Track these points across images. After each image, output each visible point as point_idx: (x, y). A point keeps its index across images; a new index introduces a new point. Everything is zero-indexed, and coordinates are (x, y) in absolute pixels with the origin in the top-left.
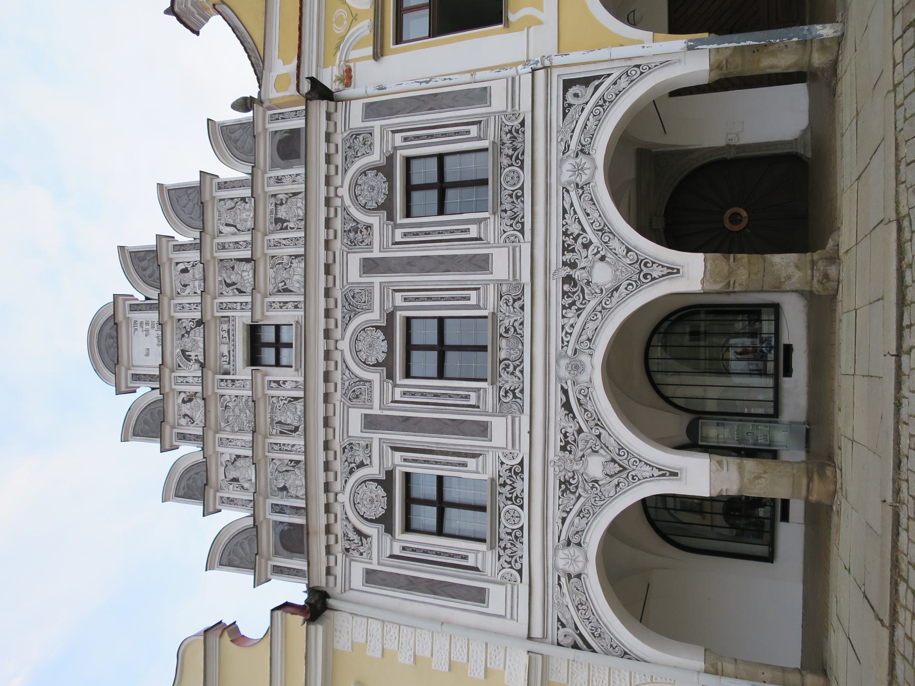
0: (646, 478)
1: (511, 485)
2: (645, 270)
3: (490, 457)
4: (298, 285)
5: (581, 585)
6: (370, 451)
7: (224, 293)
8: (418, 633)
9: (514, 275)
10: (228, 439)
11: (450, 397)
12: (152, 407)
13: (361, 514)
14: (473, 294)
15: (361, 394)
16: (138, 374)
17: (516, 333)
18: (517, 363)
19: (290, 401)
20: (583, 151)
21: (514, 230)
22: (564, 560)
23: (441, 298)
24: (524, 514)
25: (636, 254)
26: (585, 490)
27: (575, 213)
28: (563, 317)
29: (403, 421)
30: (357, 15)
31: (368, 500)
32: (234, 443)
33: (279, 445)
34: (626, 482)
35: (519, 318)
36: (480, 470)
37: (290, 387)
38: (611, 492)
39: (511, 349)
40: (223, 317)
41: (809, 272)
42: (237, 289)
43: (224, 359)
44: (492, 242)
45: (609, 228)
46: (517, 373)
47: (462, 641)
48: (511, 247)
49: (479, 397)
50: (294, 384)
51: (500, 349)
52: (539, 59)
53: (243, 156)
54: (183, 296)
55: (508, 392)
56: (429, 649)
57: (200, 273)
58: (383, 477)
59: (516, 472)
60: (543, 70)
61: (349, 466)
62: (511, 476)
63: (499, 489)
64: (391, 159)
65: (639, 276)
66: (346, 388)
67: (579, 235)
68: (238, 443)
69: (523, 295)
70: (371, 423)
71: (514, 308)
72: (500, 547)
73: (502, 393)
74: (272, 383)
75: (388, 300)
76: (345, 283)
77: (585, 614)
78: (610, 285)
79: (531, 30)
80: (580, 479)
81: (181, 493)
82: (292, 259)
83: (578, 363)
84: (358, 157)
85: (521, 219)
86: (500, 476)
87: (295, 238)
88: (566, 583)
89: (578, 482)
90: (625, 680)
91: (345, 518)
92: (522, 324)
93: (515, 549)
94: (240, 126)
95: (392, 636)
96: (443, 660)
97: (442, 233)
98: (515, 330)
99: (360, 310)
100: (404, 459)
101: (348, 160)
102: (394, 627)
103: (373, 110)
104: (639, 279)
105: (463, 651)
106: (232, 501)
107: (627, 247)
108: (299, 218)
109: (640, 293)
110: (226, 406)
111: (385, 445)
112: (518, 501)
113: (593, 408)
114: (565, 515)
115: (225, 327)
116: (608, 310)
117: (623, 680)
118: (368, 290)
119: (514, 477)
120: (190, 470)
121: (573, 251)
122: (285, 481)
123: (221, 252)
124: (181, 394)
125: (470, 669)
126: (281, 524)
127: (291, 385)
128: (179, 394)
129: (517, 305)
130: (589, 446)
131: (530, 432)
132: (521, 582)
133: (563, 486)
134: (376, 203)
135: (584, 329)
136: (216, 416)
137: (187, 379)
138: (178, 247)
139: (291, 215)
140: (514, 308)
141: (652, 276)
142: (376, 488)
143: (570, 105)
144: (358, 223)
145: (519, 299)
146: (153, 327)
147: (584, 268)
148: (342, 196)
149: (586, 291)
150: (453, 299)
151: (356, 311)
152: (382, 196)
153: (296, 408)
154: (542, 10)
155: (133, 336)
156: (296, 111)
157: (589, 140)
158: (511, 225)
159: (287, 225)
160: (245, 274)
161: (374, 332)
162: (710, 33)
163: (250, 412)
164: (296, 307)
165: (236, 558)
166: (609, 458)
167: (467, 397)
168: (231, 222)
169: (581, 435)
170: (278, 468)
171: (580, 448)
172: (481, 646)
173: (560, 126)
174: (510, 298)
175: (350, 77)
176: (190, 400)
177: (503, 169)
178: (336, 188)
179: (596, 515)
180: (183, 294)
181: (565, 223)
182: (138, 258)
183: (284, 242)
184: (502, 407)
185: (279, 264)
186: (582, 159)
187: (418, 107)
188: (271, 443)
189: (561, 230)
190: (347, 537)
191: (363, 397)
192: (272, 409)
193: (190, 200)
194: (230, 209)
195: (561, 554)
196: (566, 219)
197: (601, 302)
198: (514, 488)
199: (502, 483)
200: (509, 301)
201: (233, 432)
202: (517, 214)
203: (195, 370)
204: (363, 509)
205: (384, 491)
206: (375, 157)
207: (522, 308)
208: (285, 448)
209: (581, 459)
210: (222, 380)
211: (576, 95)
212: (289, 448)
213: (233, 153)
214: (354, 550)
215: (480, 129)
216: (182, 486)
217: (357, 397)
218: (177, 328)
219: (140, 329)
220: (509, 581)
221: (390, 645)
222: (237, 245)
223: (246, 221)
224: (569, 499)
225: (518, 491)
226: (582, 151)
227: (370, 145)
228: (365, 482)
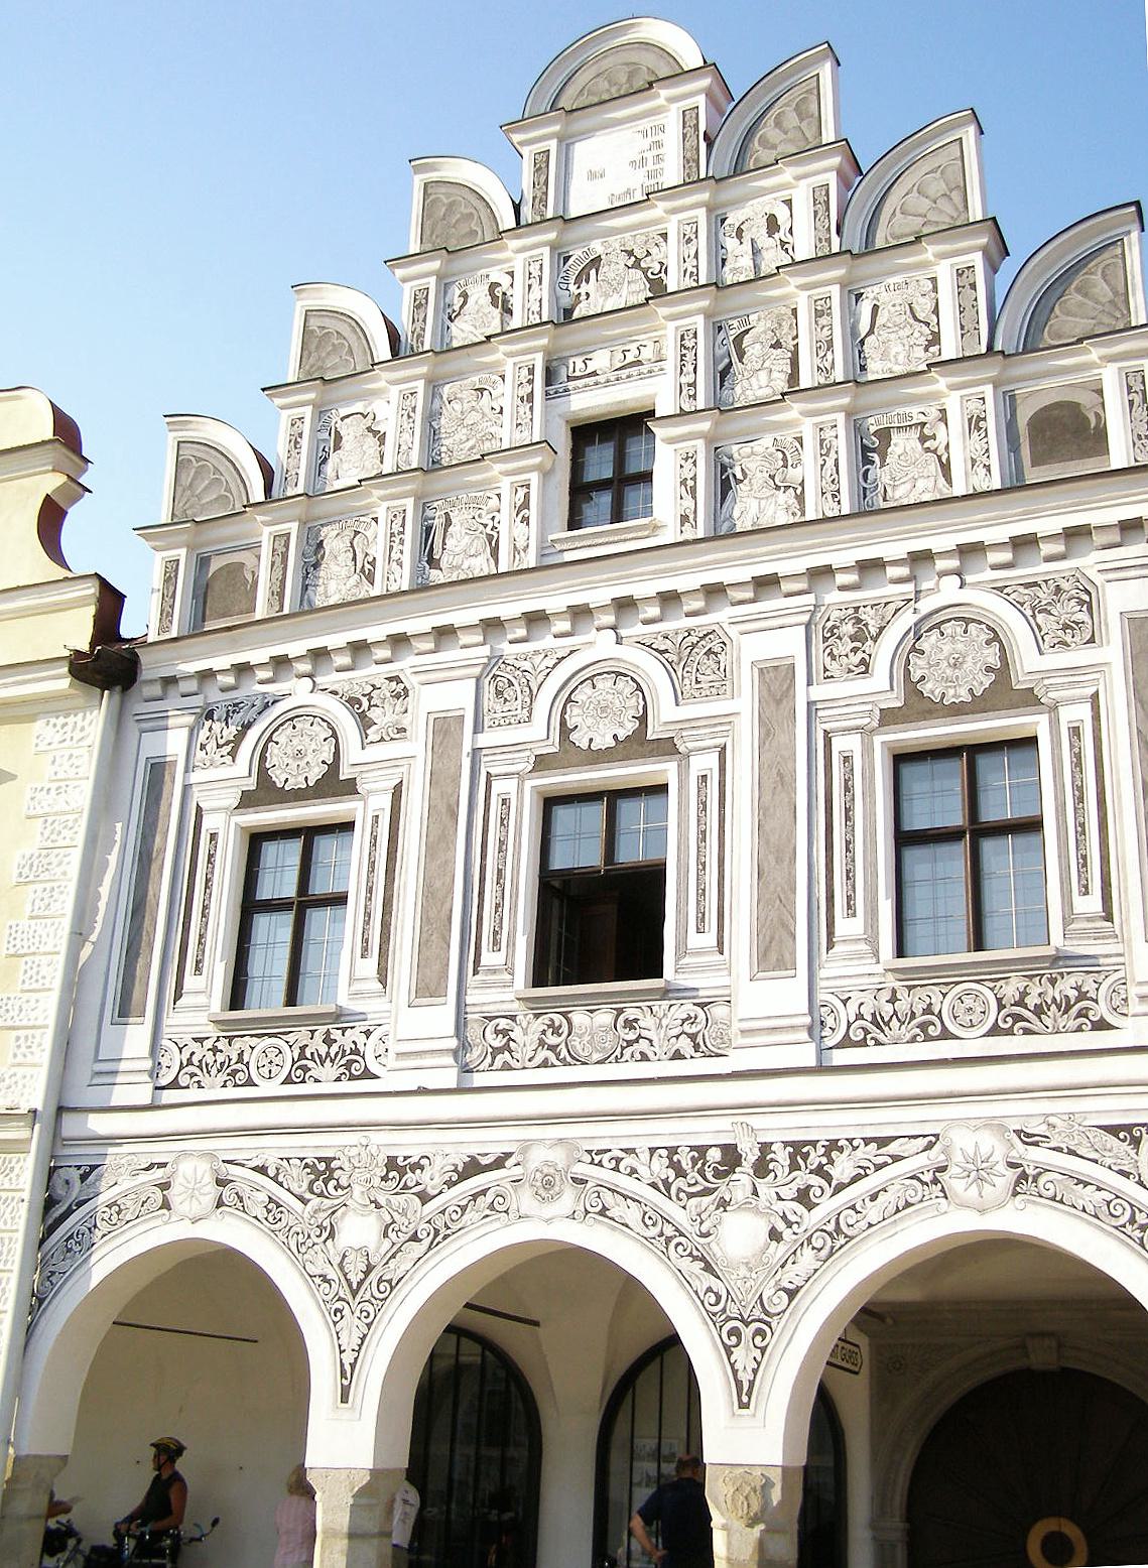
0: (339, 1338)
2: (747, 1332)
5: (151, 1210)
7: (722, 335)
11: (497, 906)
12: (484, 213)
13: (275, 735)
14: (710, 939)
17: (625, 1044)
18: (564, 1053)
20: (1023, 1179)
21: (849, 1025)
22: (192, 1174)
27: (879, 1167)
28: (652, 1150)
29: (449, 806)
36: (357, 986)
38: (313, 1269)
49: (495, 972)
58: (345, 773)
59: (353, 1066)
61: (364, 695)
64: (1029, 699)
65: (736, 1319)
67: (828, 1178)
68: (406, 436)
71: (677, 1037)
73: (503, 1023)
77: (103, 1219)
78: (719, 1254)
80: (336, 1202)
82: (795, 489)
83: (557, 1189)
85: (872, 1038)
91: (266, 701)
92: (644, 1057)
93: (214, 1071)
94: (1121, 290)
98: (630, 1043)
99: (680, 674)
101: (1026, 591)
106: (296, 442)
107: (798, 1289)
108: (889, 489)
112: (299, 1072)
113: (469, 1223)
114: (272, 1172)
116: (665, 1250)
118: (722, 684)
119: (343, 1062)
127: (521, 536)
129: (685, 1045)
130: (396, 1216)
131: (422, 1091)
133: (322, 1166)
134: (923, 678)
135: (625, 1197)
137: (535, 282)
138: (822, 199)
140: (677, 1037)
142: (324, 762)
145: (696, 1047)
147: (755, 1193)
149: (707, 1200)
152: (937, 691)
155: (631, 131)
157: (1050, 1193)
158: (860, 1016)
160: (763, 375)
161: (632, 712)
163: (469, 450)
164: (684, 519)
165: (192, 474)
168: (880, 321)
169: (417, 1199)
171: (392, 1198)
173: (1085, 1119)
177: (991, 985)
179: (272, 1234)
181: (855, 1143)
185: (785, 459)
189: (840, 1134)
191: (498, 708)
193: (935, 203)
197: (682, 1235)
199: (332, 1037)
200: (692, 1023)
202: (886, 1029)
206: (1029, 662)
207: (678, 1056)
209: (372, 1202)
210: (531, 371)
212: (395, 556)
213: (1055, 286)
215: (1089, 920)
216: (327, 322)
217: (499, 693)
219: (650, 140)
223: (884, 356)
225: (316, 1071)
226: (1024, 1176)
228: (335, 735)
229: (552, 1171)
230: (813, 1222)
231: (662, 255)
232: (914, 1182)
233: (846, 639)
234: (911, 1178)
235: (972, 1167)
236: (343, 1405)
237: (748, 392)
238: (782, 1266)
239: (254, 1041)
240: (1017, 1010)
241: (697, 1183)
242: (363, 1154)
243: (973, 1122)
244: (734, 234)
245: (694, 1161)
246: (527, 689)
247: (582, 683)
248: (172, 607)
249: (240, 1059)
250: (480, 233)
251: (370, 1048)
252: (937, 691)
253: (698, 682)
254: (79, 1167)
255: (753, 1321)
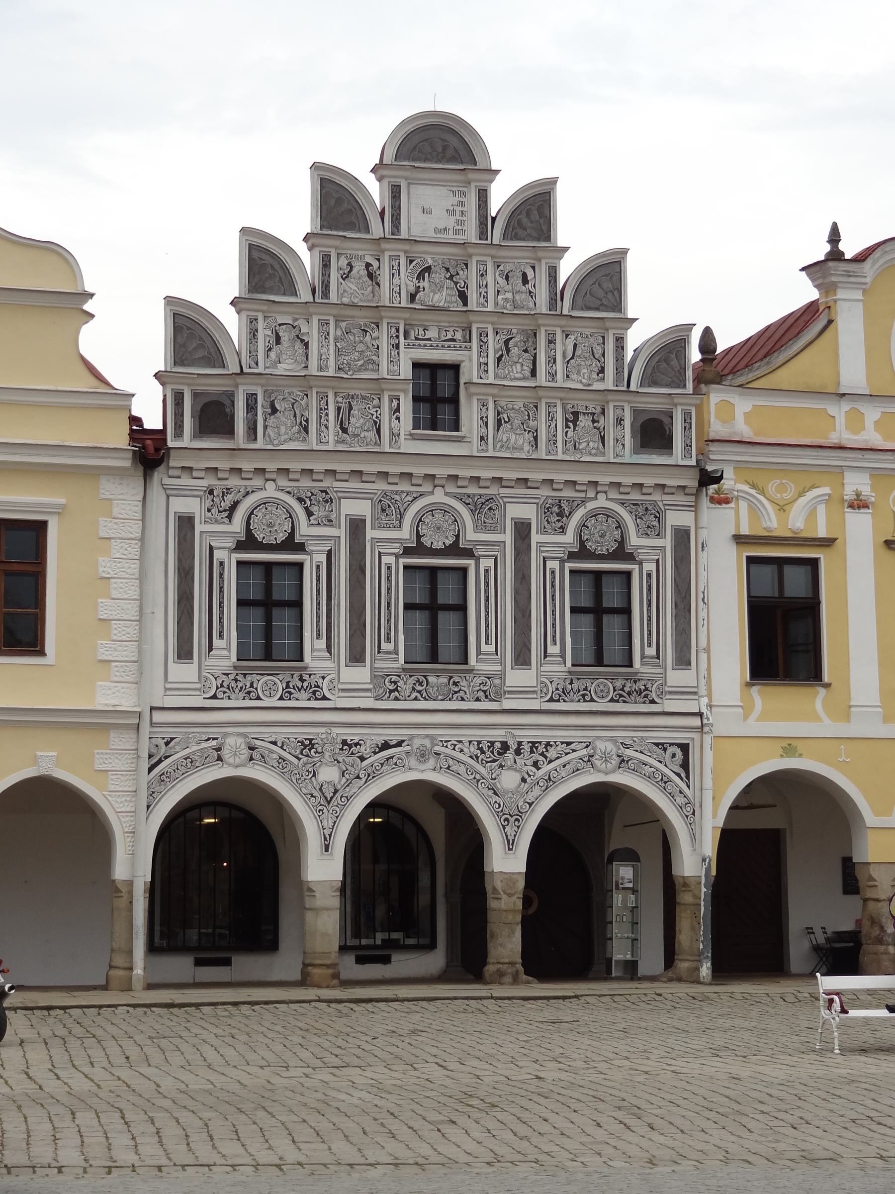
0: (322, 823)
1: (302, 687)
2: (512, 820)
3: (329, 664)
4: (504, 439)
6: (325, 525)
7: (498, 337)
8: (134, 582)
9: (510, 692)
10: (328, 334)
11: (388, 621)
12: (359, 213)
13: (255, 511)
14: (491, 648)
15: (387, 515)
16: (400, 196)
19: (375, 423)
20: (623, 761)
21: (553, 692)
23: (488, 612)
24: (274, 702)
25: (527, 812)
26: (305, 764)
27: (567, 754)
28: (470, 742)
29: (360, 567)
30: (784, 511)
31: (271, 521)
32: (324, 343)
33: (326, 407)
34: (316, 803)
35: (468, 696)
36: (315, 654)
37: (393, 426)
39: (438, 688)
40: (470, 331)
41: (506, 960)
42: (502, 355)
43: (421, 332)
44: (542, 669)
45: (551, 786)
46: (415, 694)
47: (135, 634)
48: (536, 689)
50: (396, 431)
51: (438, 676)
52: (711, 721)
53: (649, 371)
54: (495, 274)
55: (395, 685)
56: (119, 596)
57: (521, 302)
59: (316, 693)
60: (700, 724)
61: (306, 497)
62: (311, 687)
63: (297, 674)
64: (630, 557)
66: (393, 496)
67: (546, 757)
68: (324, 350)
69: (490, 701)
70: (357, 527)
71: (478, 691)
72: (237, 674)
73: (394, 678)
74: (397, 402)
75: (487, 550)
76: (505, 500)
77: (182, 765)
78: (499, 787)
79: (740, 710)
80: (317, 759)
81: (256, 254)
82: (533, 433)
83: (427, 757)
84: (636, 519)
85: (562, 699)
86: (310, 675)
87: (556, 441)
88: (211, 746)
89: (313, 757)
90: (122, 807)
91: (247, 490)
92: (463, 699)
93: (237, 691)
94: (683, 367)
95: (126, 550)
96: (111, 613)
97: (553, 614)
98: (456, 692)
100: (319, 566)
101: (633, 507)
102: (137, 553)
103: (682, 537)
104: (504, 814)
105: (124, 635)
106: (254, 335)
107: (533, 802)
108: (577, 444)
109: (491, 815)
110: (366, 331)
111: (332, 542)
112: (287, 694)
113: (385, 771)
114: (279, 744)
115: (459, 336)
117: (121, 805)
119: (311, 691)
120: (283, 269)
121: (532, 752)
122: (283, 412)
123: (546, 336)
124: (378, 263)
125: (107, 644)
126: (230, 402)
128: (376, 259)
129: (481, 694)
130: (347, 766)
132: (204, 698)
133: (307, 742)
134: (587, 540)
135: (459, 762)
136: (353, 317)
137: (396, 275)
139: (581, 433)
140: (478, 691)
141: (508, 825)
143: (665, 750)
144: (567, 517)
146: (458, 222)
147: (515, 762)
148: (597, 499)
149: (494, 764)
150: (487, 626)
151: (476, 511)
153: (368, 431)
154: (758, 719)
155: (447, 188)
156: (691, 446)
157: (633, 768)
158: (557, 689)
159: (570, 428)
161: (452, 532)
162: (716, 877)
163: (360, 366)
164: (482, 438)
166: (338, 787)
167: (388, 640)
168: (578, 352)
169: (359, 760)
170: (297, 403)
171: (345, 759)
172: (133, 656)
173: (647, 740)
174: (487, 688)
175: (720, 502)
176: (371, 276)
177: (611, 681)
178: (606, 493)
179: (282, 774)
180: (497, 273)
181: (557, 744)
182: (541, 205)
183: (553, 425)
184: (379, 678)
185: (529, 415)
186: (615, 761)
187: (679, 590)
188: (327, 396)
189: (552, 741)
190: (227, 493)
192: (365, 398)
194: (592, 350)
195: (240, 741)
196: (562, 744)
197: (484, 779)
198: (300, 690)
201: (336, 339)
202: (568, 695)
203: (406, 285)
204: (260, 514)
205: (282, 541)
206: (634, 540)
207: (478, 700)
208: (323, 416)
209: (335, 760)
210: (398, 330)
211: (674, 755)
212: (324, 422)
213: (655, 355)
214: (213, 501)
215: (652, 658)
216: (264, 256)
217: (383, 510)
218: (456, 260)
219: (456, 200)
220: (204, 685)
221: (116, 547)
222: (552, 361)
223: (578, 373)
224: (296, 749)
225: (296, 694)
226: (623, 761)
227: (647, 534)
228: (291, 517)
229: (425, 749)
230: (540, 775)
231: (465, 277)
232: (580, 760)
233: (554, 514)
234: (580, 759)
235: (603, 755)
236: (326, 853)
237: (511, 374)
238: (527, 793)
239: (259, 677)
240: (621, 692)
241: (490, 757)
242: (330, 738)
243: (605, 738)
244: (504, 277)
245: (489, 747)
246: (398, 510)
247: (427, 512)
248: (182, 422)
249: (252, 685)
250: (357, 225)
251: (325, 685)
252: (593, 547)
253: (485, 523)
254: (163, 738)
255: (515, 815)
